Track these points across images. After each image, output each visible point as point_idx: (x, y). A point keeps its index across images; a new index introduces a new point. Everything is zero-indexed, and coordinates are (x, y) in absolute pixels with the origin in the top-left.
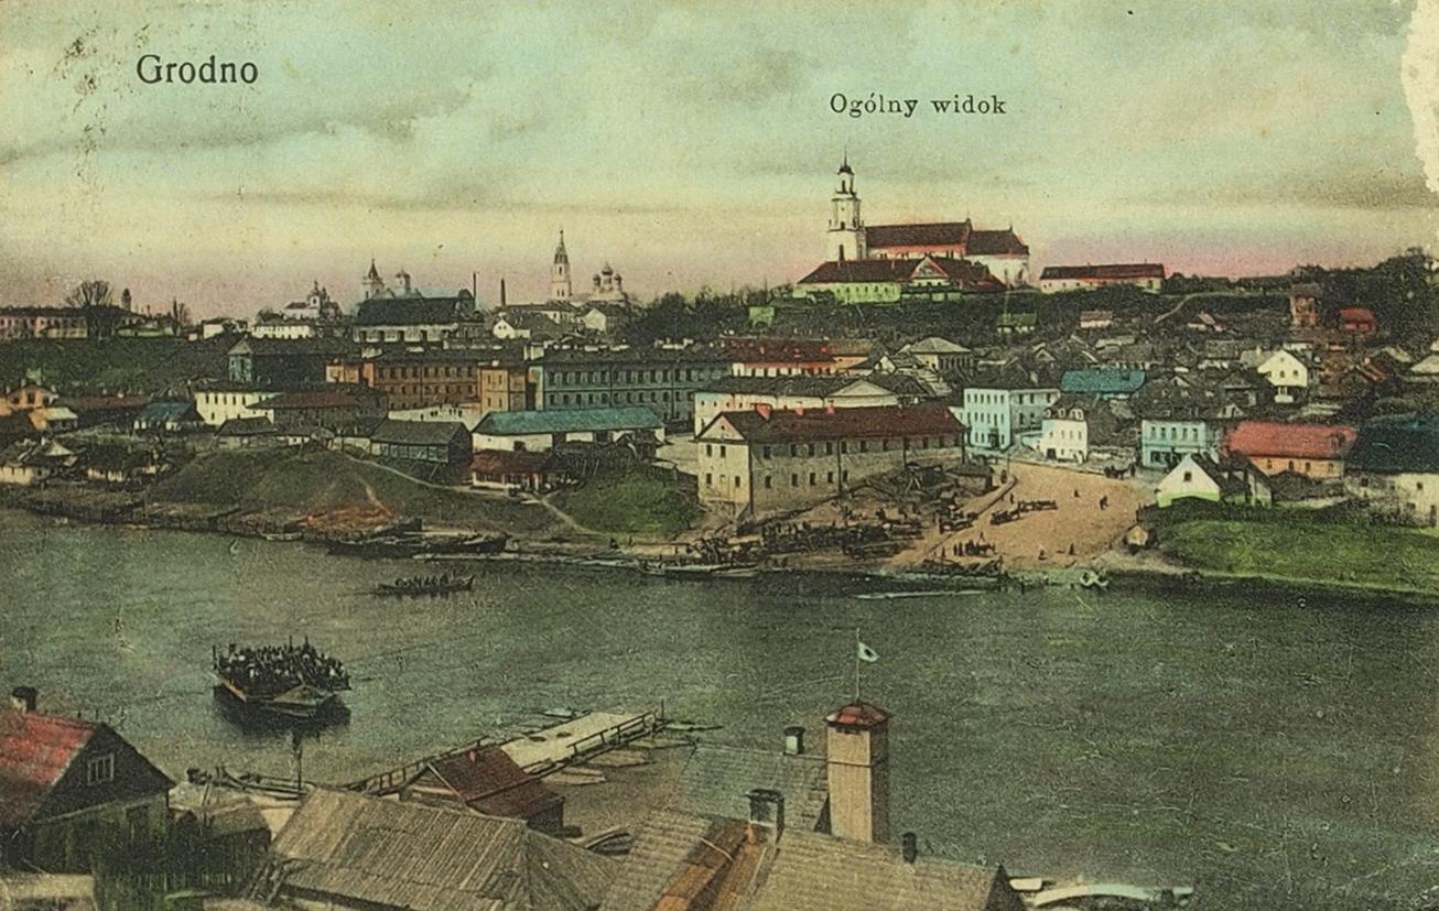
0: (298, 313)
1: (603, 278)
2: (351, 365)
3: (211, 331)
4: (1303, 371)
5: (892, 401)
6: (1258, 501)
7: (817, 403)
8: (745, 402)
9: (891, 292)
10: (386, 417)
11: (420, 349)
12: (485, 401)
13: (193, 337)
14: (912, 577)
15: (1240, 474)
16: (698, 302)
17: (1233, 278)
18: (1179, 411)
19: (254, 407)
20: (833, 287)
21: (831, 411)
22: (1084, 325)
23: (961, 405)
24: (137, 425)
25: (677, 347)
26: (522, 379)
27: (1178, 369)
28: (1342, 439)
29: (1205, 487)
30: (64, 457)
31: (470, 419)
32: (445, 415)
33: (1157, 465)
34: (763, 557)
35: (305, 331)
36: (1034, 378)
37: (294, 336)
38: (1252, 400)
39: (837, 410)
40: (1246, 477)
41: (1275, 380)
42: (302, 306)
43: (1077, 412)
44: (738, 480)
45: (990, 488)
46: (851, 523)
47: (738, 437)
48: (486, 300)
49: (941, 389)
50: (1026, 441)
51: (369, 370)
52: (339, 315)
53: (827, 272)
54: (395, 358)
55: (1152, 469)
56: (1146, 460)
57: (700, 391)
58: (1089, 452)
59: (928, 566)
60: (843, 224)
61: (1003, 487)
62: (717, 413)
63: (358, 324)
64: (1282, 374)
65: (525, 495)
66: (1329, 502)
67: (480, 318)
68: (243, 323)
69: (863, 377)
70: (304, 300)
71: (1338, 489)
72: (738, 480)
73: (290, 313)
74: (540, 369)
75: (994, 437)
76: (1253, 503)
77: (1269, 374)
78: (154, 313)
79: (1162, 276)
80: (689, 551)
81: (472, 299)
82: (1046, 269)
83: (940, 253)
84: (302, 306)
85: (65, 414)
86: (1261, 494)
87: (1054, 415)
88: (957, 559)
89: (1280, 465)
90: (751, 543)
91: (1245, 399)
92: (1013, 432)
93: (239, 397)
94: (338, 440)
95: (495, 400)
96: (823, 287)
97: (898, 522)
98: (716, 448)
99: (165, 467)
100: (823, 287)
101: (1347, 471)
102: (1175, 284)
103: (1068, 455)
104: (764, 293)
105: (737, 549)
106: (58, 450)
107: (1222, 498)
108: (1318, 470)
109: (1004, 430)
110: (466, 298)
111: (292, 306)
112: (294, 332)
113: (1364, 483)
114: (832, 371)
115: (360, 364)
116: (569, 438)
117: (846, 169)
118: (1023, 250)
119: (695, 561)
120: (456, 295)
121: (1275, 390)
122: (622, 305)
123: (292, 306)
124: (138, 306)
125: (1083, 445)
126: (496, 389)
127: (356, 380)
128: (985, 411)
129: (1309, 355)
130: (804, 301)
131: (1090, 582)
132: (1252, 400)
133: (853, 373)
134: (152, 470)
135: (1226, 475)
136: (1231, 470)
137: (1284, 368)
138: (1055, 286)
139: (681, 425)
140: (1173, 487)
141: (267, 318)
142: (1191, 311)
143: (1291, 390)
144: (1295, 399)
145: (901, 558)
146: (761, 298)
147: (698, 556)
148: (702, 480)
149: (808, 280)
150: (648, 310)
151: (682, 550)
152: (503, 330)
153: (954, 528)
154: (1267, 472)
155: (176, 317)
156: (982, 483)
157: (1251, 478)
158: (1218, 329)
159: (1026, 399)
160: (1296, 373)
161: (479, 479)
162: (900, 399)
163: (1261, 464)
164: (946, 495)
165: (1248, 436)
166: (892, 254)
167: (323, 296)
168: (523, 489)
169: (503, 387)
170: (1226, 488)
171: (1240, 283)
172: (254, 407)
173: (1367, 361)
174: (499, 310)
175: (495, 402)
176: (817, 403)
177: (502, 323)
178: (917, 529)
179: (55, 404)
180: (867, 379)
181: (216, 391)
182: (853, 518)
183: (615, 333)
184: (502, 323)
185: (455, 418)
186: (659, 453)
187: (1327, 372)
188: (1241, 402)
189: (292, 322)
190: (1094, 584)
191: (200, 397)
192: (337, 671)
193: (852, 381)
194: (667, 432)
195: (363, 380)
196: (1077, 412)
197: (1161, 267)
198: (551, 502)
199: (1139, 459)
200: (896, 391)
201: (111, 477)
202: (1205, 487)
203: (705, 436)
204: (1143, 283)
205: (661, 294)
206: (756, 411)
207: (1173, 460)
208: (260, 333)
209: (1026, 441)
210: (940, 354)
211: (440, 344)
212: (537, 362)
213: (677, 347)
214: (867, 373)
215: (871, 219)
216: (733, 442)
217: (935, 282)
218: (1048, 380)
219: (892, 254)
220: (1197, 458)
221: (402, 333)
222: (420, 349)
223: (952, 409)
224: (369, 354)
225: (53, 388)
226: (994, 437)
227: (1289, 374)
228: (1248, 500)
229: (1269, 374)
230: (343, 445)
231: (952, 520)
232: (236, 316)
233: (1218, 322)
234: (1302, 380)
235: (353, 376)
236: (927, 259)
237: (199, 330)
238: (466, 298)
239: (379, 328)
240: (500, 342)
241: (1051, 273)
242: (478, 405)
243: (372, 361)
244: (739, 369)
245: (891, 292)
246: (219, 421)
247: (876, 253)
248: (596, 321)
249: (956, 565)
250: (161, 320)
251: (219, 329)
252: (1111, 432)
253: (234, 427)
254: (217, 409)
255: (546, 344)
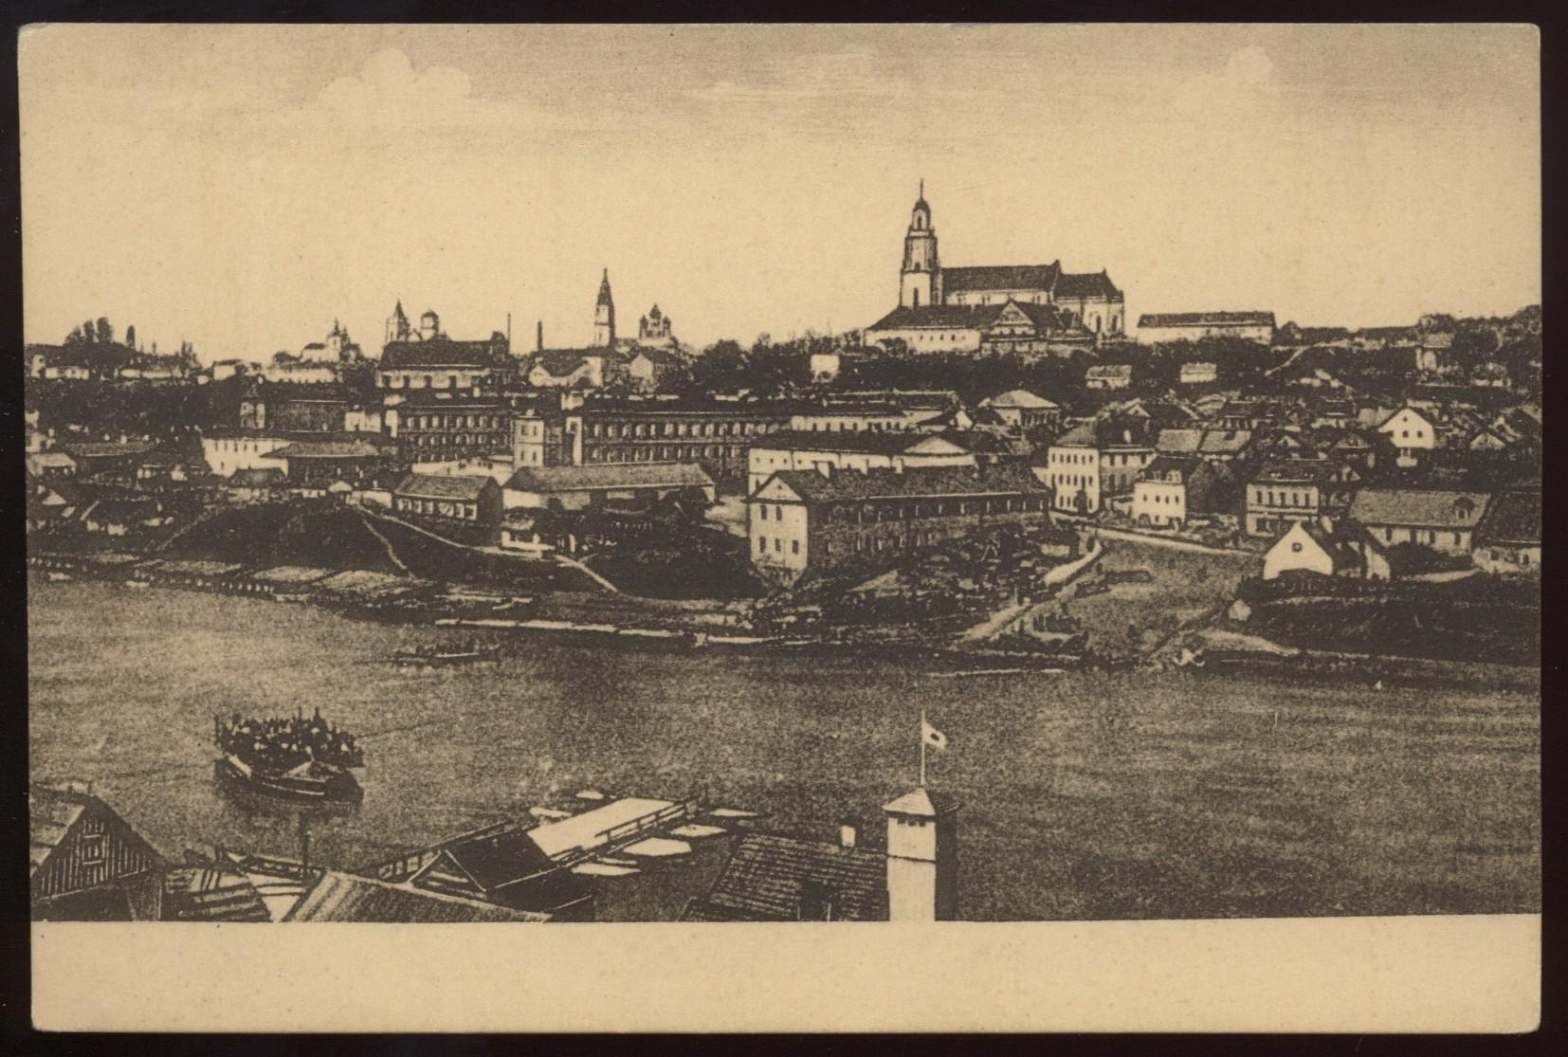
0: (316, 355)
1: (651, 321)
2: (369, 412)
3: (223, 373)
4: (1427, 428)
5: (969, 460)
6: (1375, 576)
7: (880, 461)
8: (805, 460)
9: (968, 340)
10: (409, 471)
11: (446, 396)
12: (518, 455)
13: (202, 380)
14: (988, 652)
15: (1355, 545)
16: (758, 348)
17: (1352, 328)
18: (1290, 475)
19: (265, 456)
20: (905, 334)
21: (899, 470)
22: (1185, 379)
23: (1044, 464)
24: (140, 473)
25: (732, 398)
26: (558, 431)
27: (1288, 428)
28: (1471, 506)
29: (1320, 561)
30: (63, 508)
31: (501, 474)
32: (475, 469)
33: (1264, 534)
34: (814, 629)
35: (325, 376)
36: (1127, 436)
37: (312, 381)
38: (1371, 461)
39: (906, 469)
40: (1362, 548)
41: (1398, 441)
42: (320, 346)
43: (1176, 475)
44: (796, 544)
45: (1074, 556)
46: (920, 593)
47: (797, 498)
48: (522, 345)
49: (1023, 446)
50: (1117, 505)
51: (392, 419)
52: (360, 357)
53: (903, 317)
54: (418, 401)
55: (1259, 539)
56: (1251, 527)
57: (756, 445)
58: (1188, 517)
59: (1005, 642)
60: (918, 265)
61: (1089, 557)
62: (771, 471)
63: (383, 368)
64: (1405, 434)
65: (560, 558)
66: (1456, 575)
67: (514, 362)
68: (256, 366)
69: (934, 434)
70: (318, 340)
71: (1464, 563)
72: (796, 544)
73: (308, 354)
74: (578, 420)
75: (1081, 499)
76: (1369, 576)
77: (1390, 434)
78: (161, 351)
79: (1274, 325)
80: (738, 621)
81: (506, 343)
82: (1143, 317)
83: (1024, 296)
84: (320, 346)
85: (61, 460)
86: (1379, 566)
87: (1148, 475)
88: (1037, 634)
89: (1401, 536)
90: (807, 614)
91: (1363, 461)
92: (1103, 495)
93: (251, 445)
94: (357, 494)
95: (530, 450)
96: (892, 334)
97: (973, 592)
98: (771, 508)
99: (169, 520)
100: (892, 334)
101: (1475, 543)
102: (1285, 334)
103: (1163, 521)
104: (827, 340)
105: (792, 619)
106: (55, 499)
107: (1335, 571)
108: (1444, 541)
109: (1093, 492)
110: (500, 340)
111: (311, 347)
112: (311, 376)
113: (1495, 557)
114: (902, 426)
115: (382, 411)
116: (609, 496)
117: (922, 205)
118: (1114, 295)
119: (745, 633)
120: (488, 337)
121: (1397, 452)
122: (672, 351)
123: (311, 347)
124: (143, 343)
125: (1179, 511)
126: (531, 440)
127: (377, 429)
128: (1072, 469)
129: (1436, 412)
130: (873, 350)
131: (1184, 662)
132: (1371, 461)
133: (925, 429)
134: (155, 522)
135: (1339, 546)
136: (1345, 541)
137: (1410, 430)
138: (1150, 337)
139: (733, 482)
140: (1279, 560)
141: (282, 359)
142: (1304, 367)
143: (1416, 452)
144: (1419, 462)
145: (979, 632)
146: (824, 346)
147: (749, 626)
148: (755, 545)
149: (881, 325)
150: (699, 358)
151: (731, 620)
152: (540, 377)
153: (1035, 600)
154: (1386, 543)
155: (183, 358)
156: (1063, 550)
157: (1368, 552)
158: (1335, 384)
159: (1118, 459)
160: (1420, 434)
161: (513, 539)
162: (977, 458)
163: (1380, 534)
164: (1025, 564)
165: (1369, 505)
166: (973, 299)
167: (344, 337)
168: (557, 551)
169: (540, 438)
170: (1344, 559)
171: (1360, 333)
172: (265, 456)
173: (1501, 421)
174: (534, 355)
175: (529, 457)
176: (880, 461)
177: (539, 369)
178: (996, 602)
179: (54, 450)
180: (943, 436)
181: (226, 438)
182: (922, 588)
183: (666, 382)
184: (539, 369)
185: (484, 471)
186: (709, 514)
187: (1456, 431)
188: (1359, 465)
189: (310, 365)
190: (1189, 664)
191: (208, 444)
192: (350, 745)
193: (923, 438)
194: (718, 494)
195: (386, 429)
196: (1176, 475)
197: (1271, 316)
198: (587, 565)
199: (1243, 524)
200: (969, 451)
201: (113, 530)
202: (1320, 561)
203: (761, 496)
204: (1250, 333)
205: (714, 342)
206: (816, 471)
207: (1281, 527)
208: (277, 376)
209: (1117, 505)
210: (1023, 409)
211: (469, 391)
212: (575, 412)
213: (732, 398)
214: (940, 428)
215: (947, 261)
216: (786, 502)
217: (1018, 331)
218: (1146, 438)
219: (973, 299)
220: (1306, 526)
221: (428, 379)
222: (446, 396)
223: (1036, 470)
224: (395, 400)
225: (51, 432)
226: (1081, 499)
227: (1413, 433)
228: (1364, 571)
229: (1390, 434)
230: (362, 500)
231: (1030, 588)
232: (247, 359)
233: (1334, 376)
234: (1428, 442)
235: (374, 424)
236: (1012, 307)
237: (209, 373)
238: (500, 340)
239: (404, 373)
240: (534, 389)
241: (1145, 321)
242: (508, 458)
243: (394, 407)
244: (799, 423)
245: (968, 340)
246: (229, 472)
247: (953, 300)
248: (642, 369)
249: (1034, 640)
250: (168, 362)
251: (230, 371)
252: (1216, 494)
253: (242, 476)
254: (223, 456)
255: (587, 392)
